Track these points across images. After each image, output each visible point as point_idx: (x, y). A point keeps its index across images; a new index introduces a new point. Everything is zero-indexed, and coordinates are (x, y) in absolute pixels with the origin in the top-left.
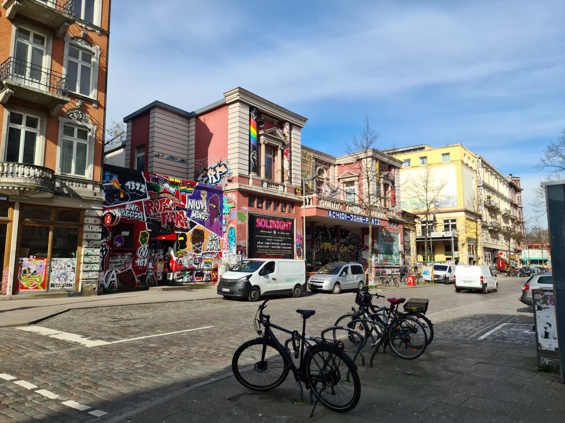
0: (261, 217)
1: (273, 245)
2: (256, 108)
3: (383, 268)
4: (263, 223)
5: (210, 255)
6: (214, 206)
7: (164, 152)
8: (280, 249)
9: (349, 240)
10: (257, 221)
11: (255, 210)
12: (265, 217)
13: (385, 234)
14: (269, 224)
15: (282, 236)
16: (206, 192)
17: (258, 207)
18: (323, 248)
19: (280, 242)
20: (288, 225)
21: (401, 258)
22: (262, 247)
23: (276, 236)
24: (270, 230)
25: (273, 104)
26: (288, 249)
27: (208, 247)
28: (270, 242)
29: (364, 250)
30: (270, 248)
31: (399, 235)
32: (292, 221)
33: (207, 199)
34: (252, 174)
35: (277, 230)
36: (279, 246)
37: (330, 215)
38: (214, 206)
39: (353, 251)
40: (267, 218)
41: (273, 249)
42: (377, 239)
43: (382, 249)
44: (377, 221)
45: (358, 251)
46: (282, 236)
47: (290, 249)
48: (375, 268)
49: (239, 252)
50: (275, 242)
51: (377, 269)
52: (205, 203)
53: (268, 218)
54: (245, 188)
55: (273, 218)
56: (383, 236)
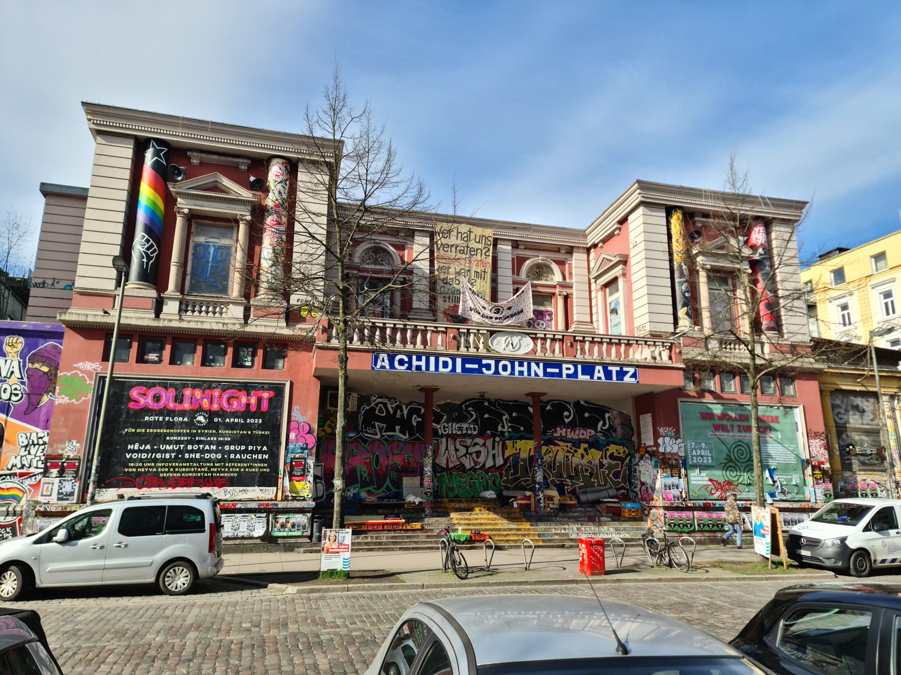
0: (149, 384)
1: (192, 451)
2: (156, 140)
3: (706, 508)
4: (157, 398)
5: (16, 479)
6: (45, 369)
7: (58, 275)
8: (219, 461)
9: (605, 433)
10: (134, 393)
11: (130, 370)
12: (165, 384)
13: (717, 410)
14: (179, 399)
15: (232, 426)
16: (21, 339)
17: (141, 359)
18: (516, 456)
19: (223, 443)
20: (259, 400)
21: (810, 480)
22: (144, 456)
23: (205, 428)
24: (182, 413)
25: (207, 122)
26: (256, 461)
27: (17, 462)
28: (178, 442)
29: (641, 458)
30: (176, 459)
31: (798, 413)
32: (278, 389)
33: (23, 355)
34: (133, 286)
35: (211, 414)
36: (216, 452)
37: (386, 364)
38: (45, 369)
39: (622, 460)
40: (172, 385)
41: (190, 460)
42: (675, 424)
43: (705, 454)
44: (621, 374)
45: (630, 461)
46: (232, 426)
47: (263, 461)
48: (666, 508)
49: (55, 472)
50: (199, 442)
51: (676, 514)
52: (15, 364)
53: (179, 387)
54: (82, 319)
55: (197, 385)
56: (708, 415)
